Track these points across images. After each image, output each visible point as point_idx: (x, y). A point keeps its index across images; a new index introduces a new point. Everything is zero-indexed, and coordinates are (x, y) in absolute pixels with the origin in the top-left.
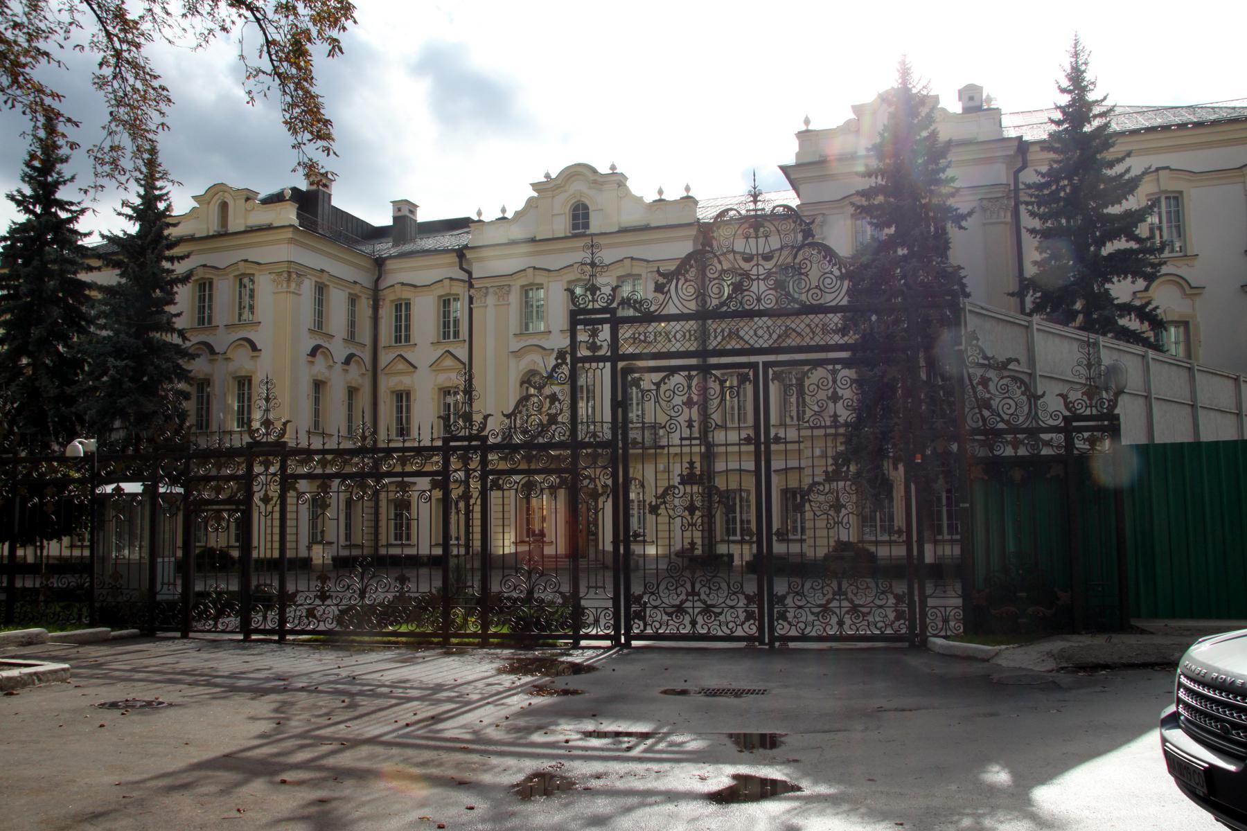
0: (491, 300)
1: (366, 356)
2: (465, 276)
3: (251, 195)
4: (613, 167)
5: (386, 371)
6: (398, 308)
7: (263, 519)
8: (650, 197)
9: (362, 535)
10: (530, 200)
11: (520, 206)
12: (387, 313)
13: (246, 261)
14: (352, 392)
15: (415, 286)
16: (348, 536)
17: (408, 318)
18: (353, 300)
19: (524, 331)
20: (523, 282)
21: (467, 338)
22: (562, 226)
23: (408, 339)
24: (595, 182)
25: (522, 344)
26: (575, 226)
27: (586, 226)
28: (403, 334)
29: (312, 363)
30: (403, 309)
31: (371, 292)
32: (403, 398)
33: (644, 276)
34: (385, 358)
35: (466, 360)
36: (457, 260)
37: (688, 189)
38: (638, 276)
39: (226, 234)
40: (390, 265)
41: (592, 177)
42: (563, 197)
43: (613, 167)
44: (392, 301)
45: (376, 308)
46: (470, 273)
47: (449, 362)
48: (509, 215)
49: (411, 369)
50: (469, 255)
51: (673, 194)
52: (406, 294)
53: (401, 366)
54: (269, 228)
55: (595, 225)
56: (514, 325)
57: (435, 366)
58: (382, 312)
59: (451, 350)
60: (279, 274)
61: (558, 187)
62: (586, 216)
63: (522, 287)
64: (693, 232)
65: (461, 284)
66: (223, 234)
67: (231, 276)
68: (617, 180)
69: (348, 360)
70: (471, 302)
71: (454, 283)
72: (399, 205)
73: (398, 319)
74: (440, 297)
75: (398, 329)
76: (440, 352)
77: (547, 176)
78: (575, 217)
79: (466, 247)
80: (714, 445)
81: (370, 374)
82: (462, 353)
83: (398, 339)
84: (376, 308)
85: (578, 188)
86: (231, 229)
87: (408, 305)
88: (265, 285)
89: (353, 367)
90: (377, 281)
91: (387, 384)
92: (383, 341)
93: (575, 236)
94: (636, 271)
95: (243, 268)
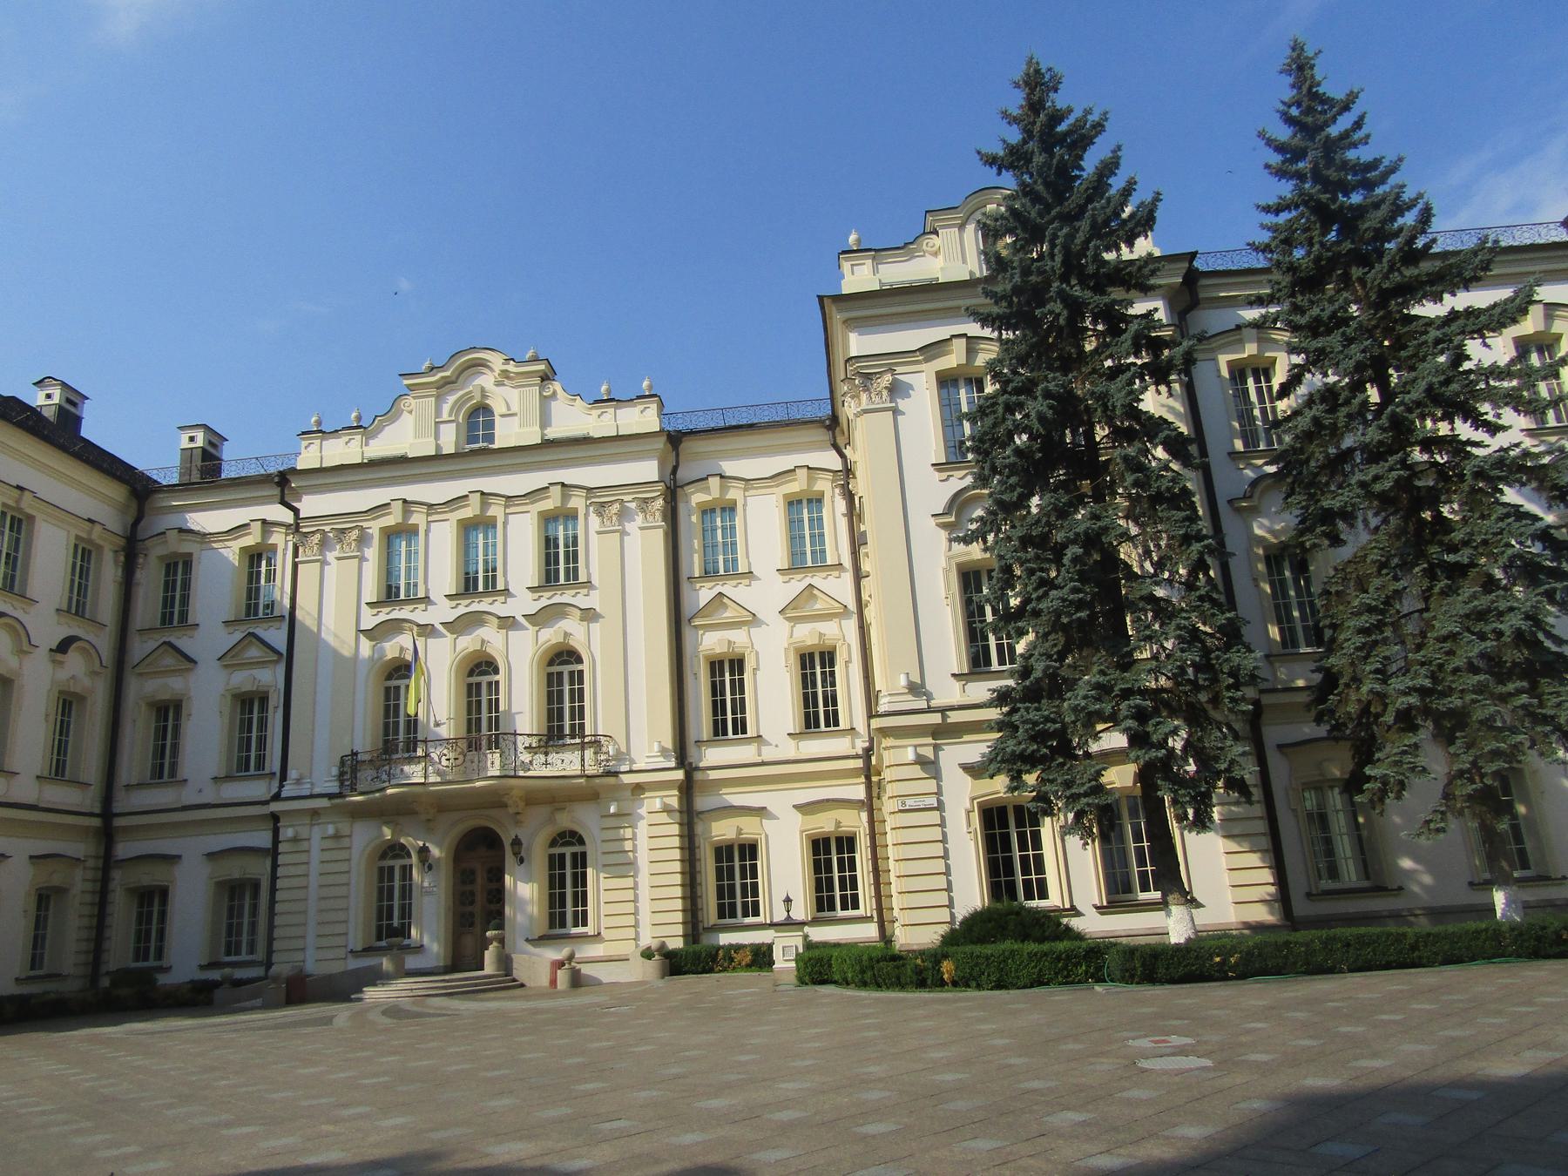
1: (104, 643)
2: (288, 517)
5: (137, 670)
9: (69, 954)
12: (150, 578)
14: (68, 704)
16: (35, 961)
17: (186, 585)
18: (84, 555)
19: (390, 595)
23: (184, 616)
26: (472, 439)
27: (490, 438)
28: (176, 611)
31: (122, 542)
32: (168, 713)
34: (140, 648)
35: (283, 648)
36: (277, 491)
44: (161, 558)
46: (296, 511)
47: (254, 652)
49: (189, 665)
53: (170, 660)
55: (507, 434)
57: (230, 659)
58: (139, 575)
62: (490, 425)
64: (661, 443)
69: (64, 646)
70: (296, 554)
73: (169, 586)
75: (168, 602)
76: (238, 636)
80: (697, 769)
83: (167, 619)
89: (75, 662)
91: (140, 690)
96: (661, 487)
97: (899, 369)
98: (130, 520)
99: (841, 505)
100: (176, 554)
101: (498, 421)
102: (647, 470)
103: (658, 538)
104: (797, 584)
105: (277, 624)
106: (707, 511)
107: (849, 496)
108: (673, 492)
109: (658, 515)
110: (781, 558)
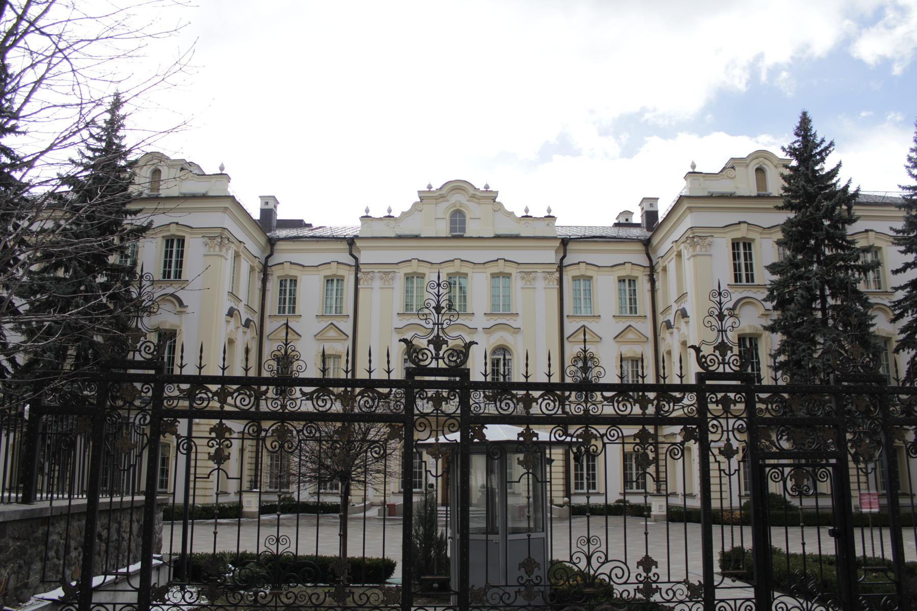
0: (377, 284)
2: (352, 261)
3: (186, 166)
4: (487, 187)
6: (282, 283)
7: (725, 480)
8: (520, 213)
10: (415, 204)
11: (407, 208)
13: (177, 223)
15: (303, 266)
20: (409, 270)
21: (351, 313)
22: (443, 229)
24: (473, 196)
25: (405, 322)
26: (452, 230)
27: (463, 229)
29: (228, 322)
30: (289, 286)
33: (513, 276)
35: (350, 332)
37: (549, 211)
38: (508, 276)
39: (157, 198)
40: (280, 246)
41: (472, 191)
42: (444, 205)
43: (487, 187)
44: (278, 277)
45: (264, 281)
47: (332, 333)
48: (396, 213)
49: (296, 337)
50: (358, 243)
51: (538, 212)
52: (294, 272)
54: (204, 197)
55: (472, 229)
56: (399, 306)
57: (318, 336)
58: (269, 285)
59: (335, 322)
60: (212, 238)
61: (442, 196)
63: (405, 274)
64: (557, 244)
65: (348, 268)
66: (157, 198)
67: (160, 239)
68: (489, 197)
71: (340, 266)
72: (266, 200)
74: (325, 277)
76: (325, 323)
77: (430, 187)
78: (453, 222)
79: (356, 237)
81: (257, 337)
82: (346, 326)
83: (282, 310)
84: (264, 281)
85: (458, 198)
86: (163, 193)
87: (294, 281)
88: (194, 249)
90: (267, 258)
92: (268, 312)
93: (454, 237)
94: (507, 270)
95: (174, 230)
96: (556, 266)
97: (715, 235)
98: (266, 255)
99: (648, 286)
100: (287, 276)
101: (468, 222)
102: (550, 256)
103: (555, 294)
104: (622, 326)
105: (345, 319)
106: (575, 279)
107: (652, 281)
108: (561, 268)
109: (556, 282)
110: (614, 309)
